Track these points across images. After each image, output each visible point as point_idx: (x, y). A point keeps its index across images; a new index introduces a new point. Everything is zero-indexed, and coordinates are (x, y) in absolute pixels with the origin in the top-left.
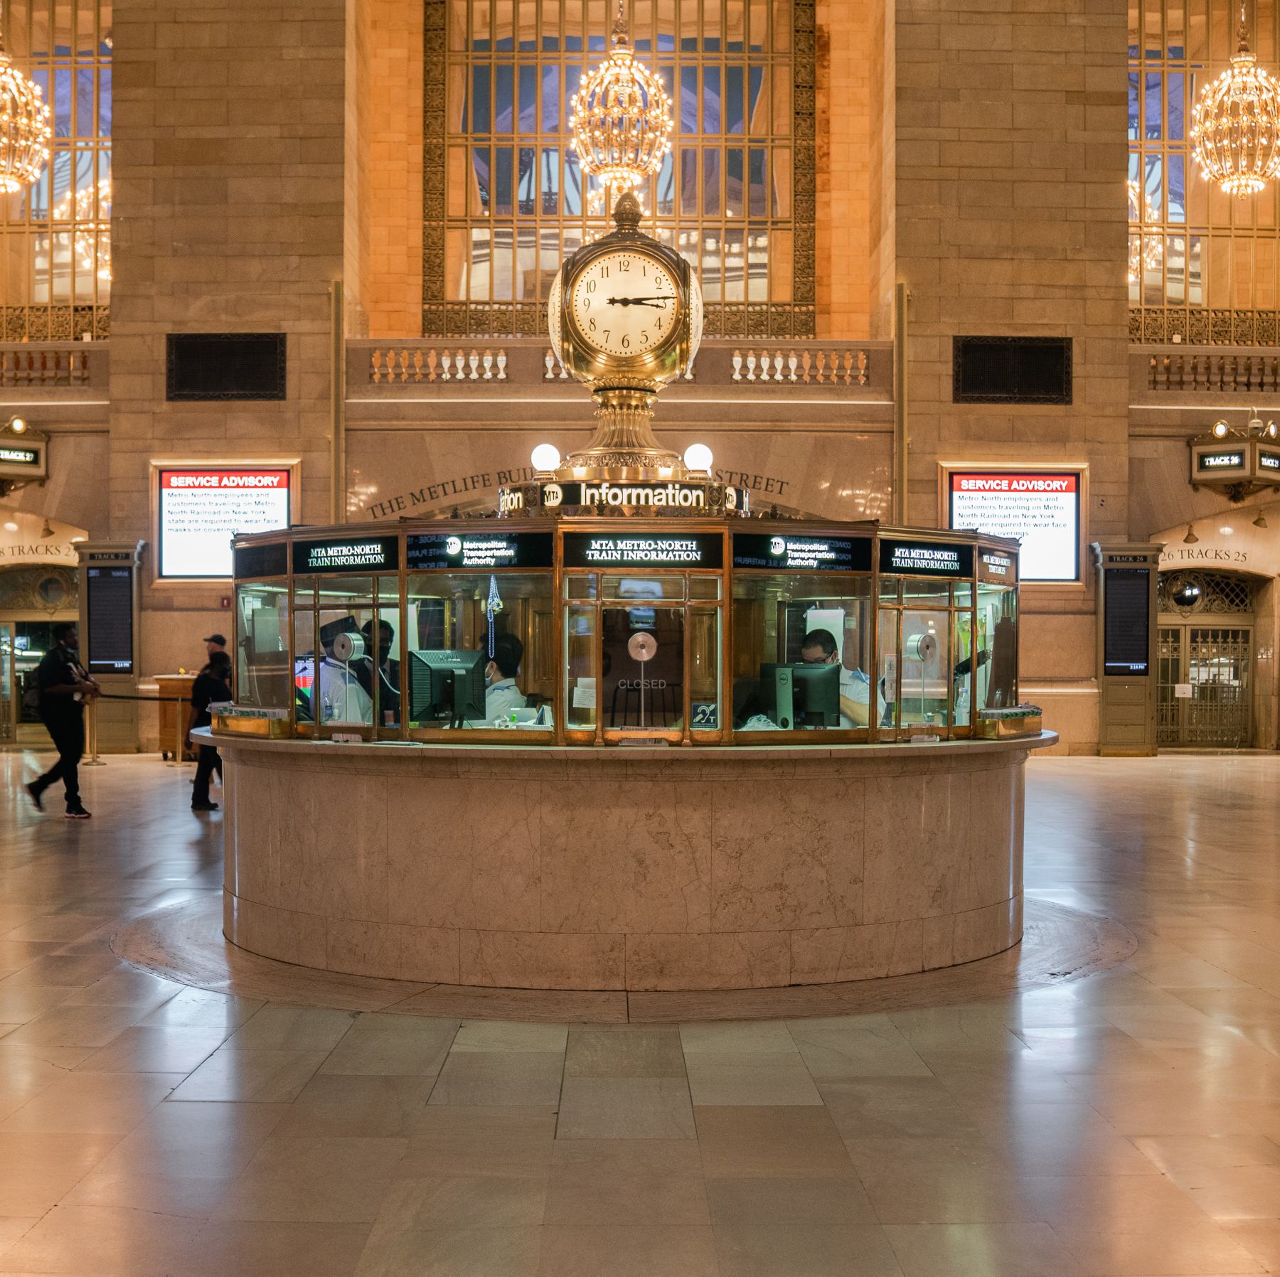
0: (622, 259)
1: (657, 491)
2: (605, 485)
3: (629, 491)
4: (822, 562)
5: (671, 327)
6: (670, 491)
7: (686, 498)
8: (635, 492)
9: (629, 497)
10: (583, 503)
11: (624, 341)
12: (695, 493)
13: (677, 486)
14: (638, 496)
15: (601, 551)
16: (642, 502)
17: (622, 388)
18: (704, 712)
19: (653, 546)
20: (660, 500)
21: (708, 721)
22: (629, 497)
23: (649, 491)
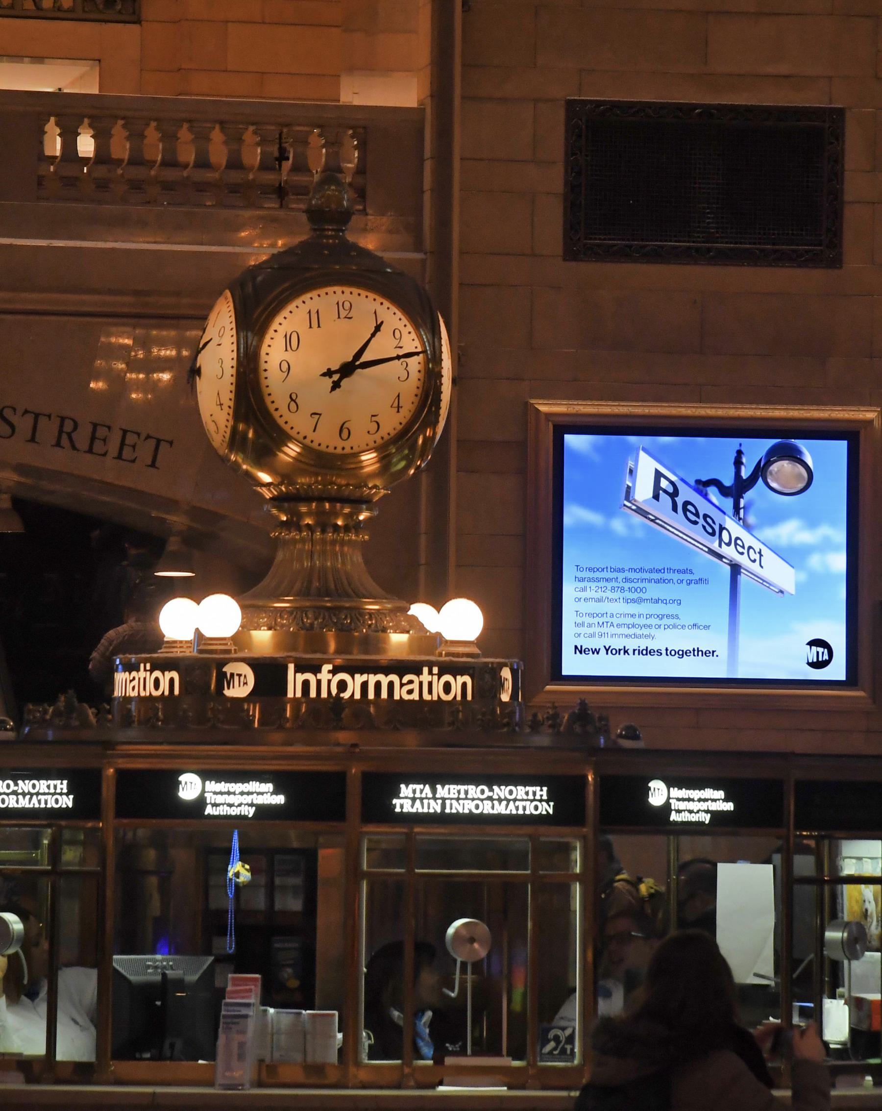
0: (341, 298)
1: (405, 679)
2: (327, 667)
3: (364, 677)
4: (715, 814)
5: (413, 408)
6: (425, 677)
7: (447, 688)
8: (372, 679)
9: (364, 686)
10: (290, 695)
11: (343, 430)
12: (461, 679)
13: (435, 670)
14: (378, 685)
15: (414, 800)
16: (384, 695)
17: (321, 499)
18: (557, 1039)
19: (487, 793)
20: (410, 692)
21: (563, 1051)
22: (364, 685)
23: (394, 678)
